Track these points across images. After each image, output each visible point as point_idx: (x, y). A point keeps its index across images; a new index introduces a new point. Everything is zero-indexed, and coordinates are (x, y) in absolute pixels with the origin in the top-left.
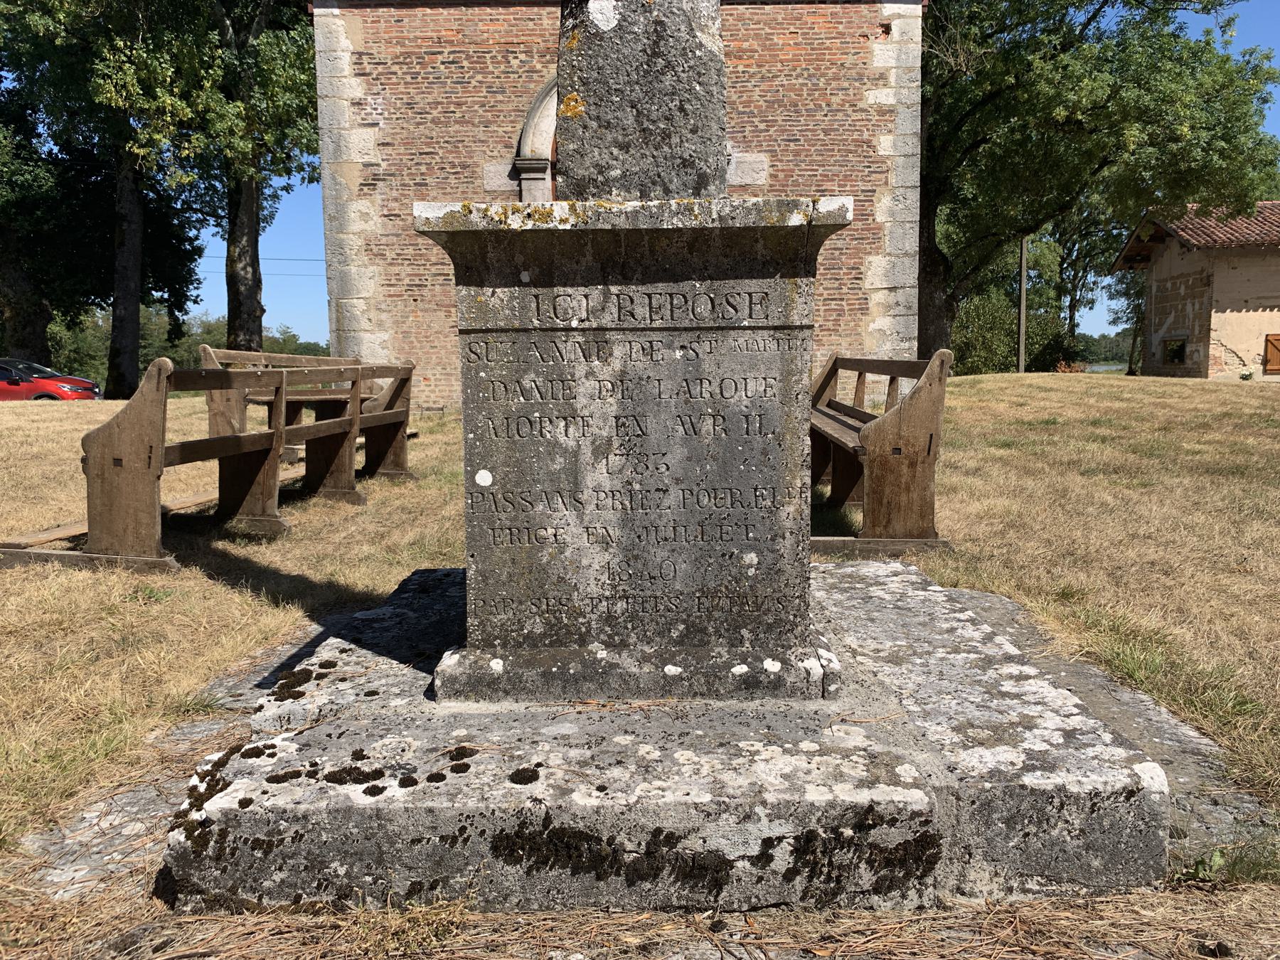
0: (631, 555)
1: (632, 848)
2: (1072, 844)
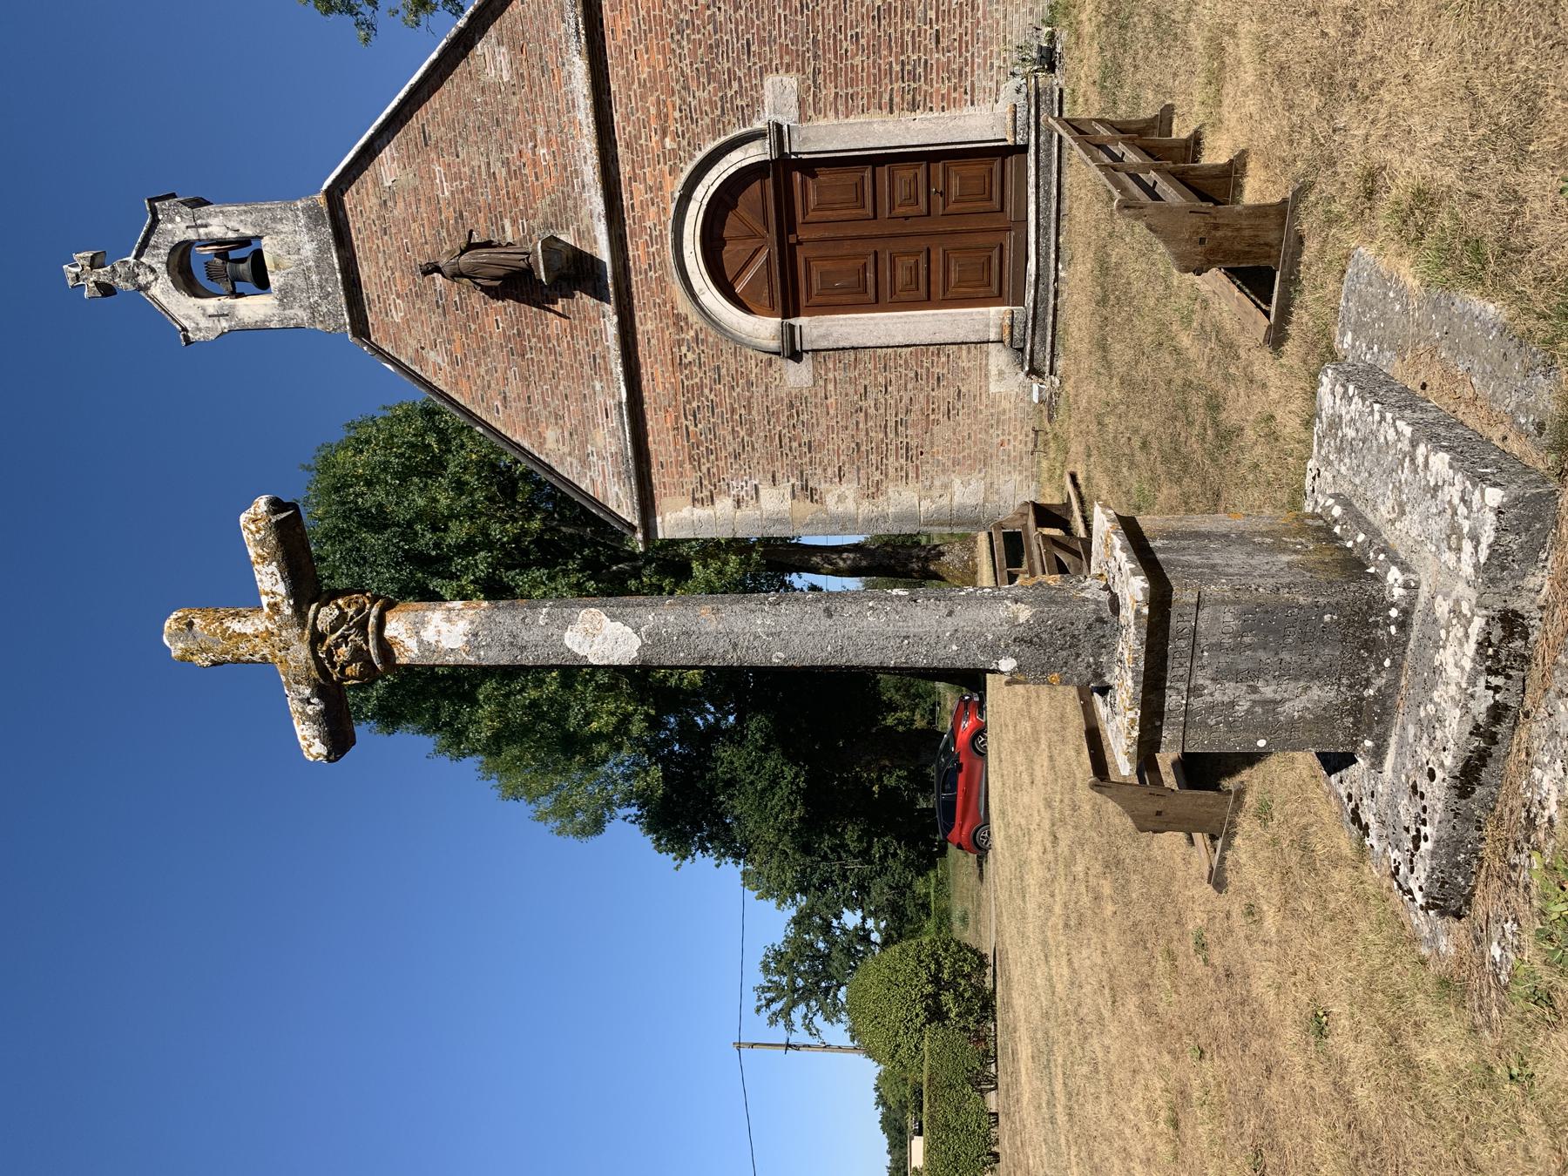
0: (1316, 676)
1: (1477, 742)
2: (1524, 538)
